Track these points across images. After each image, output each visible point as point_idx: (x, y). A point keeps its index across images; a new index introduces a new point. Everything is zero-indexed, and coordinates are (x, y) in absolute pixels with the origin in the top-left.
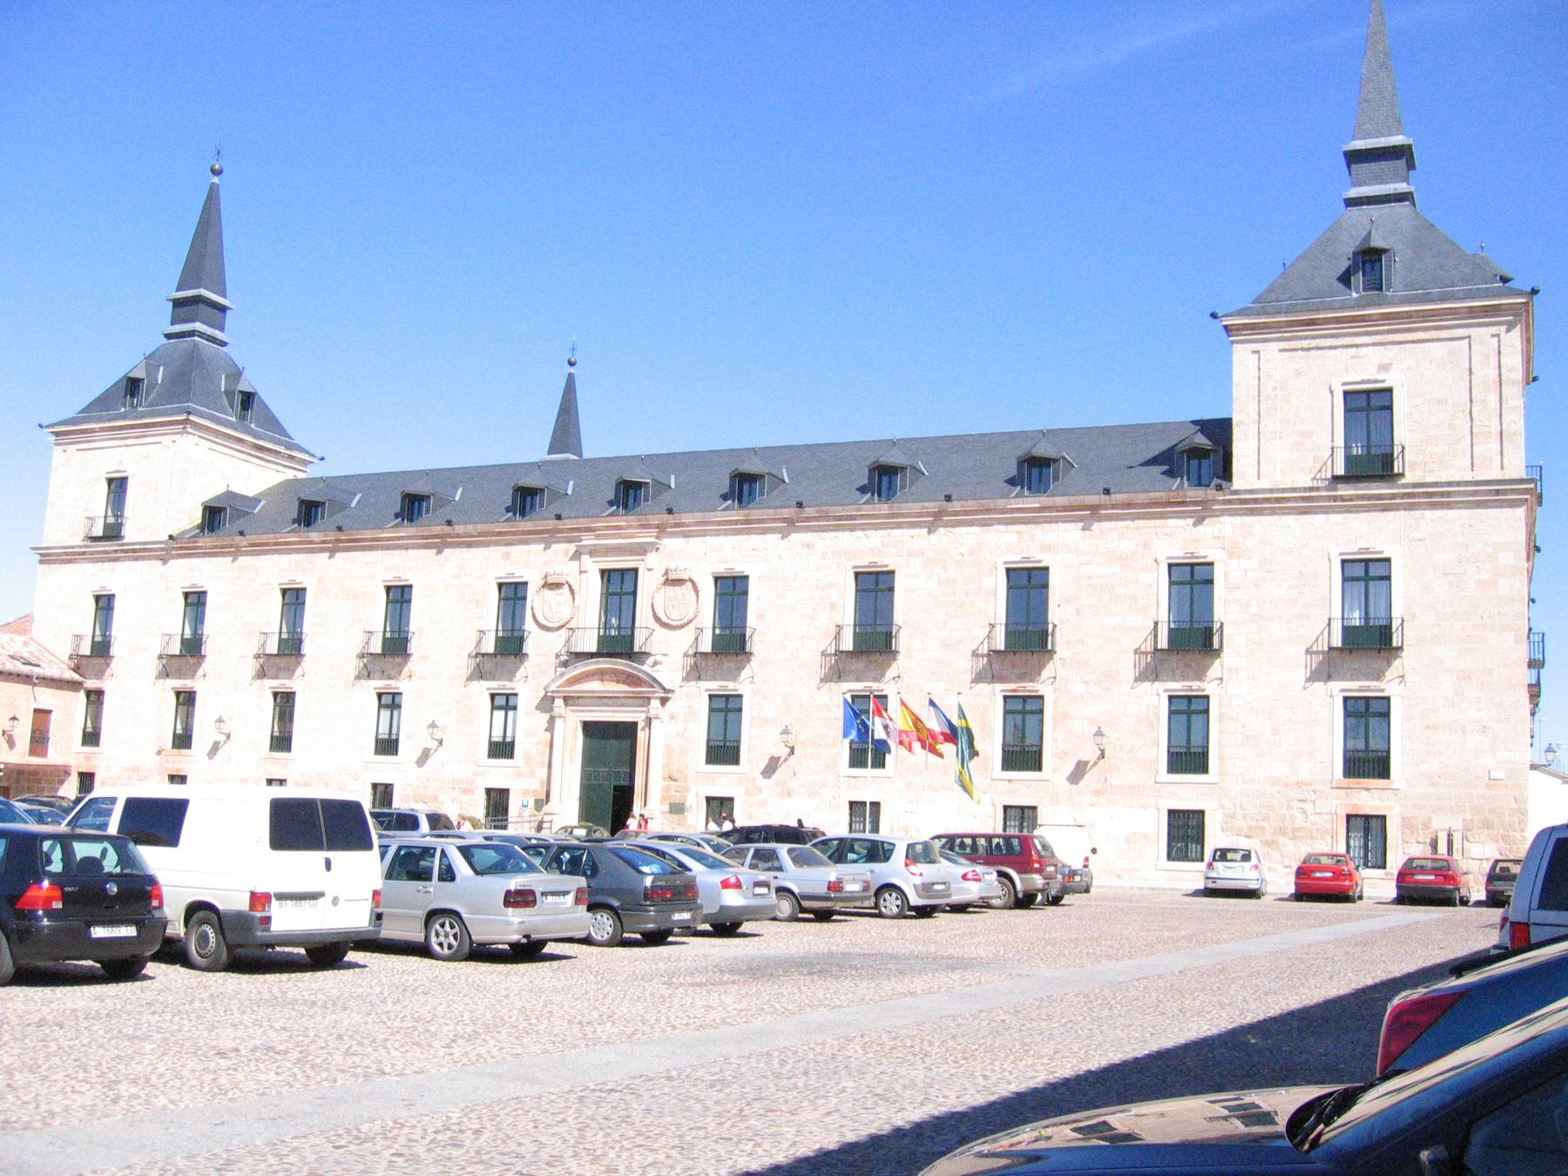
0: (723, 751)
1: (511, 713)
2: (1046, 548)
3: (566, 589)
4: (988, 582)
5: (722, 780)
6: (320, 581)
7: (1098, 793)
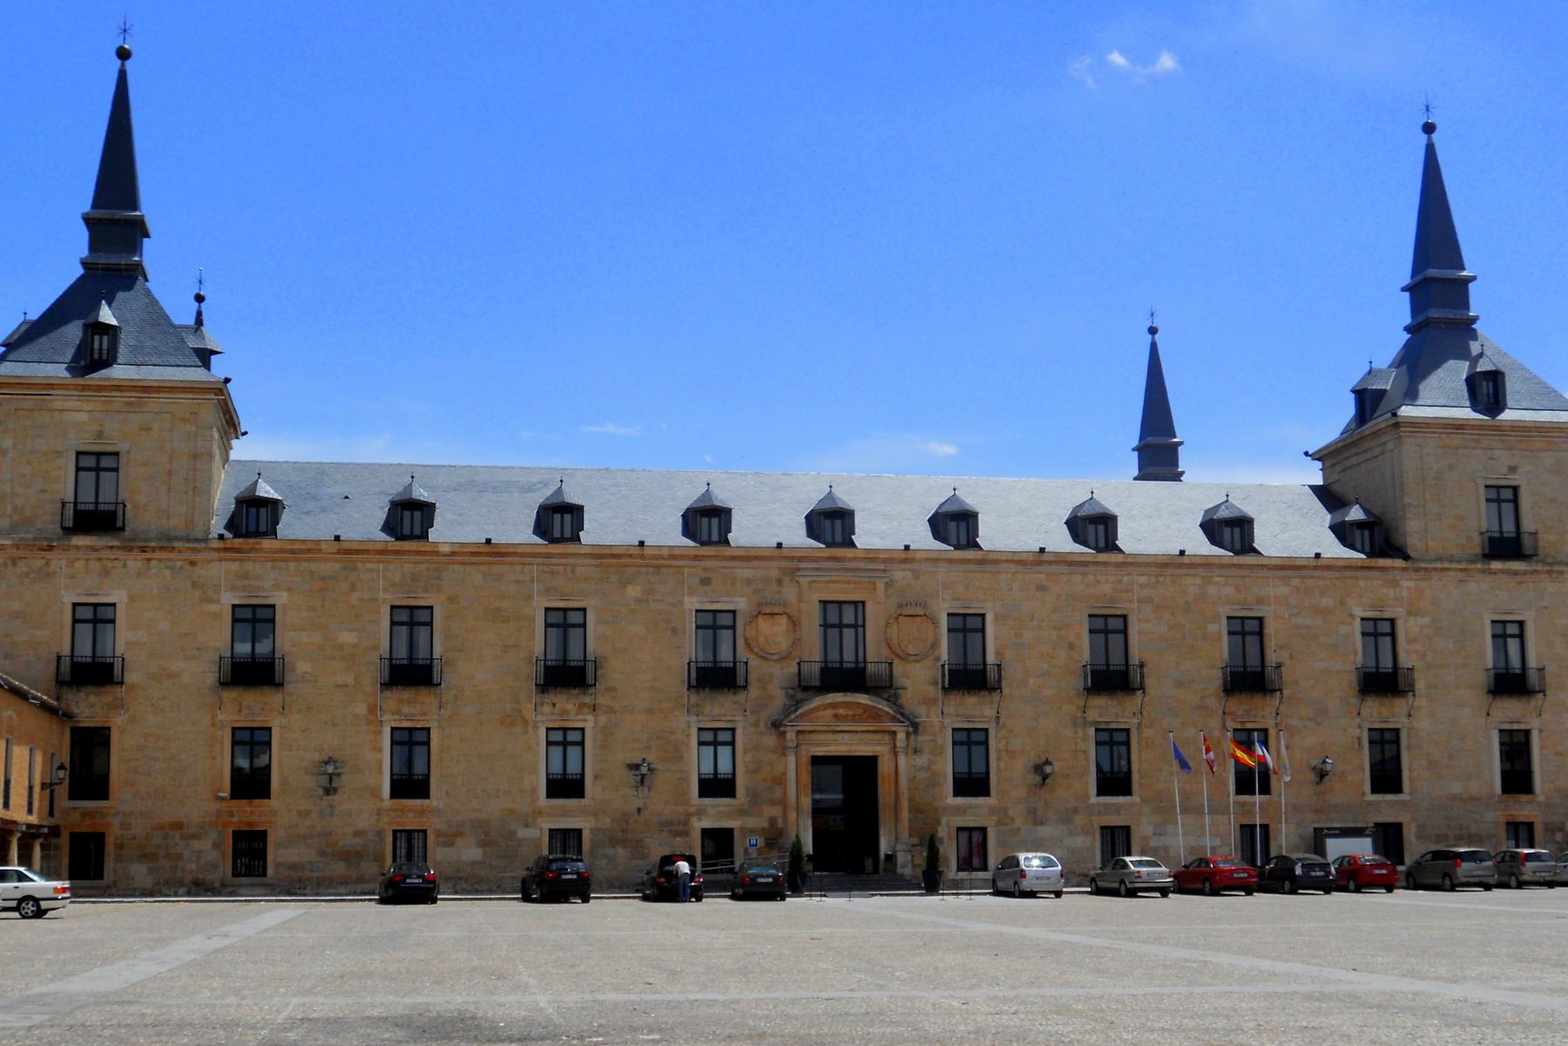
0: (972, 784)
1: (725, 752)
2: (1261, 601)
3: (784, 621)
4: (1212, 628)
5: (975, 811)
6: (451, 599)
7: (1317, 811)
